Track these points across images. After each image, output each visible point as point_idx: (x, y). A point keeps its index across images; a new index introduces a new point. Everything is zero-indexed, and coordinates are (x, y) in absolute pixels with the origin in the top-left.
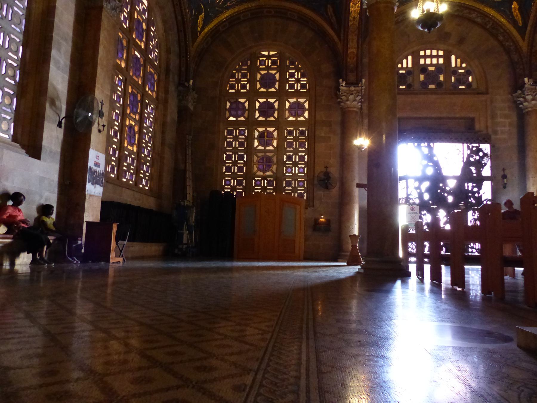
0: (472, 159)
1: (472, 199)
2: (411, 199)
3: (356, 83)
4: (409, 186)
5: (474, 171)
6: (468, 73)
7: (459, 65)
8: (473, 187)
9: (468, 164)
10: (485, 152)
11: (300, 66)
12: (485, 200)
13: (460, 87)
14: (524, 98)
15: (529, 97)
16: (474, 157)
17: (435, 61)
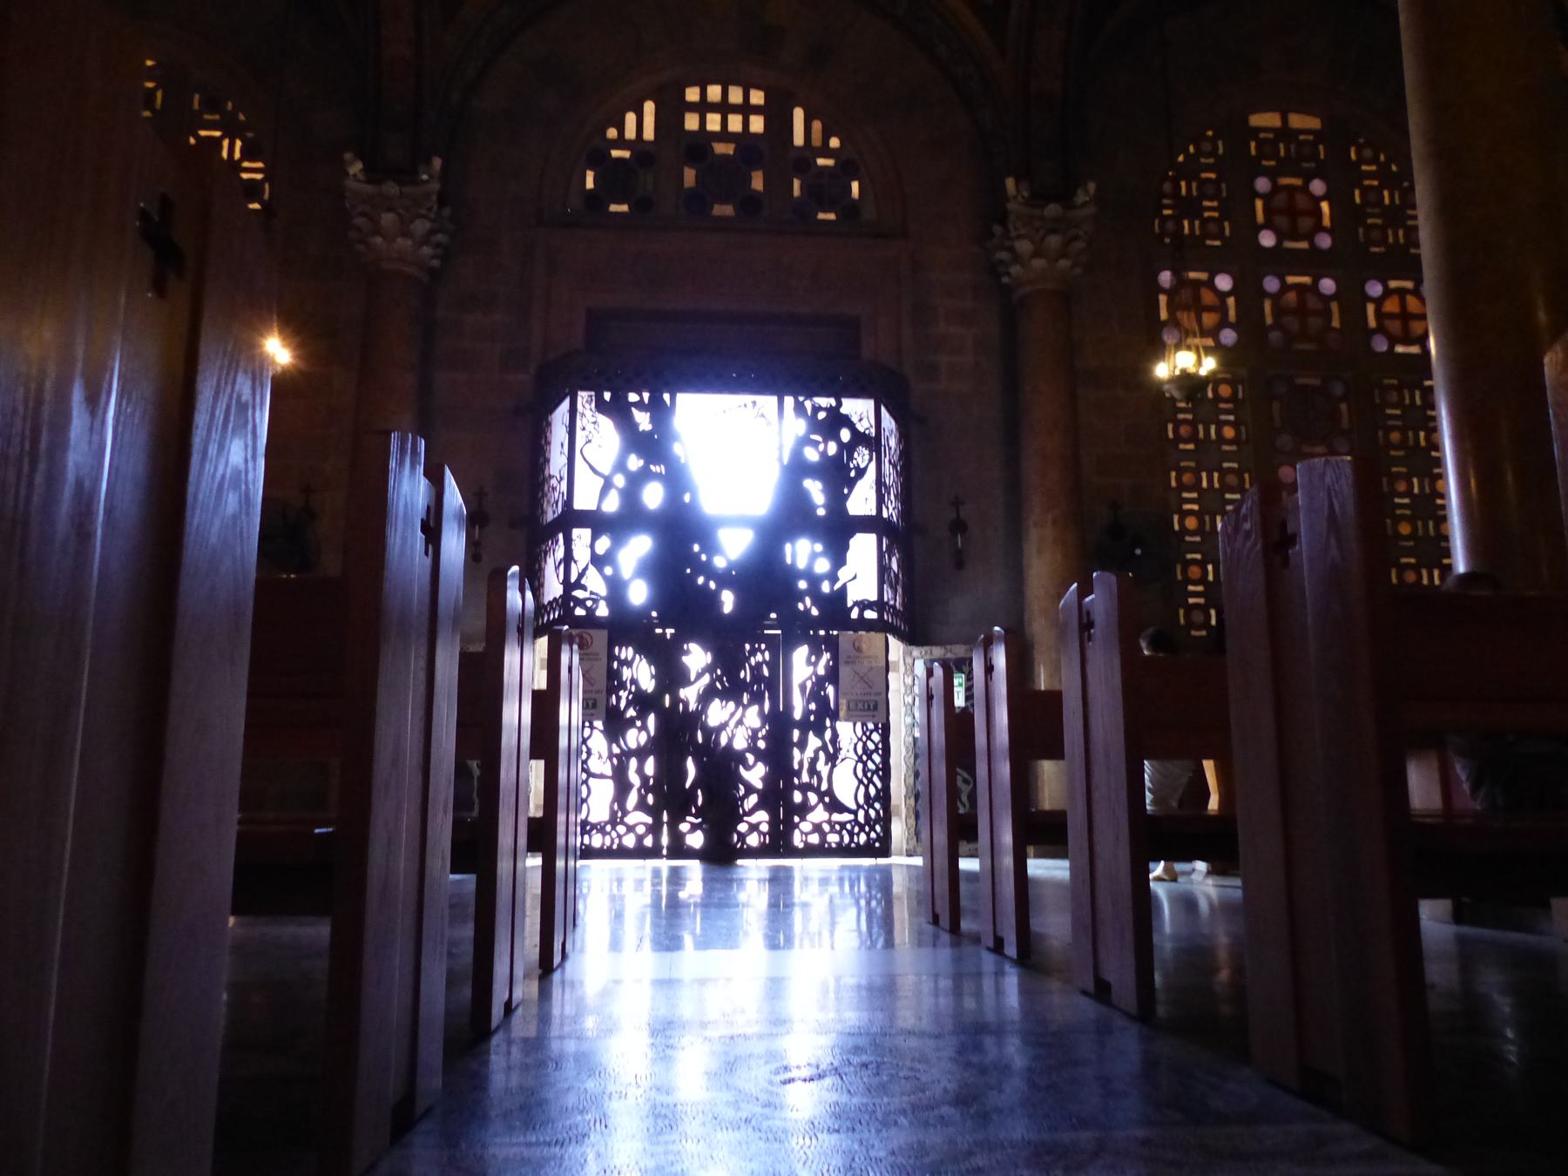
0: (812, 455)
1: (808, 601)
2: (581, 603)
3: (406, 174)
4: (576, 555)
6: (847, 167)
7: (817, 140)
8: (814, 556)
9: (797, 469)
10: (861, 428)
11: (242, 117)
12: (856, 604)
13: (821, 216)
14: (1011, 249)
15: (1024, 246)
16: (821, 447)
17: (735, 122)
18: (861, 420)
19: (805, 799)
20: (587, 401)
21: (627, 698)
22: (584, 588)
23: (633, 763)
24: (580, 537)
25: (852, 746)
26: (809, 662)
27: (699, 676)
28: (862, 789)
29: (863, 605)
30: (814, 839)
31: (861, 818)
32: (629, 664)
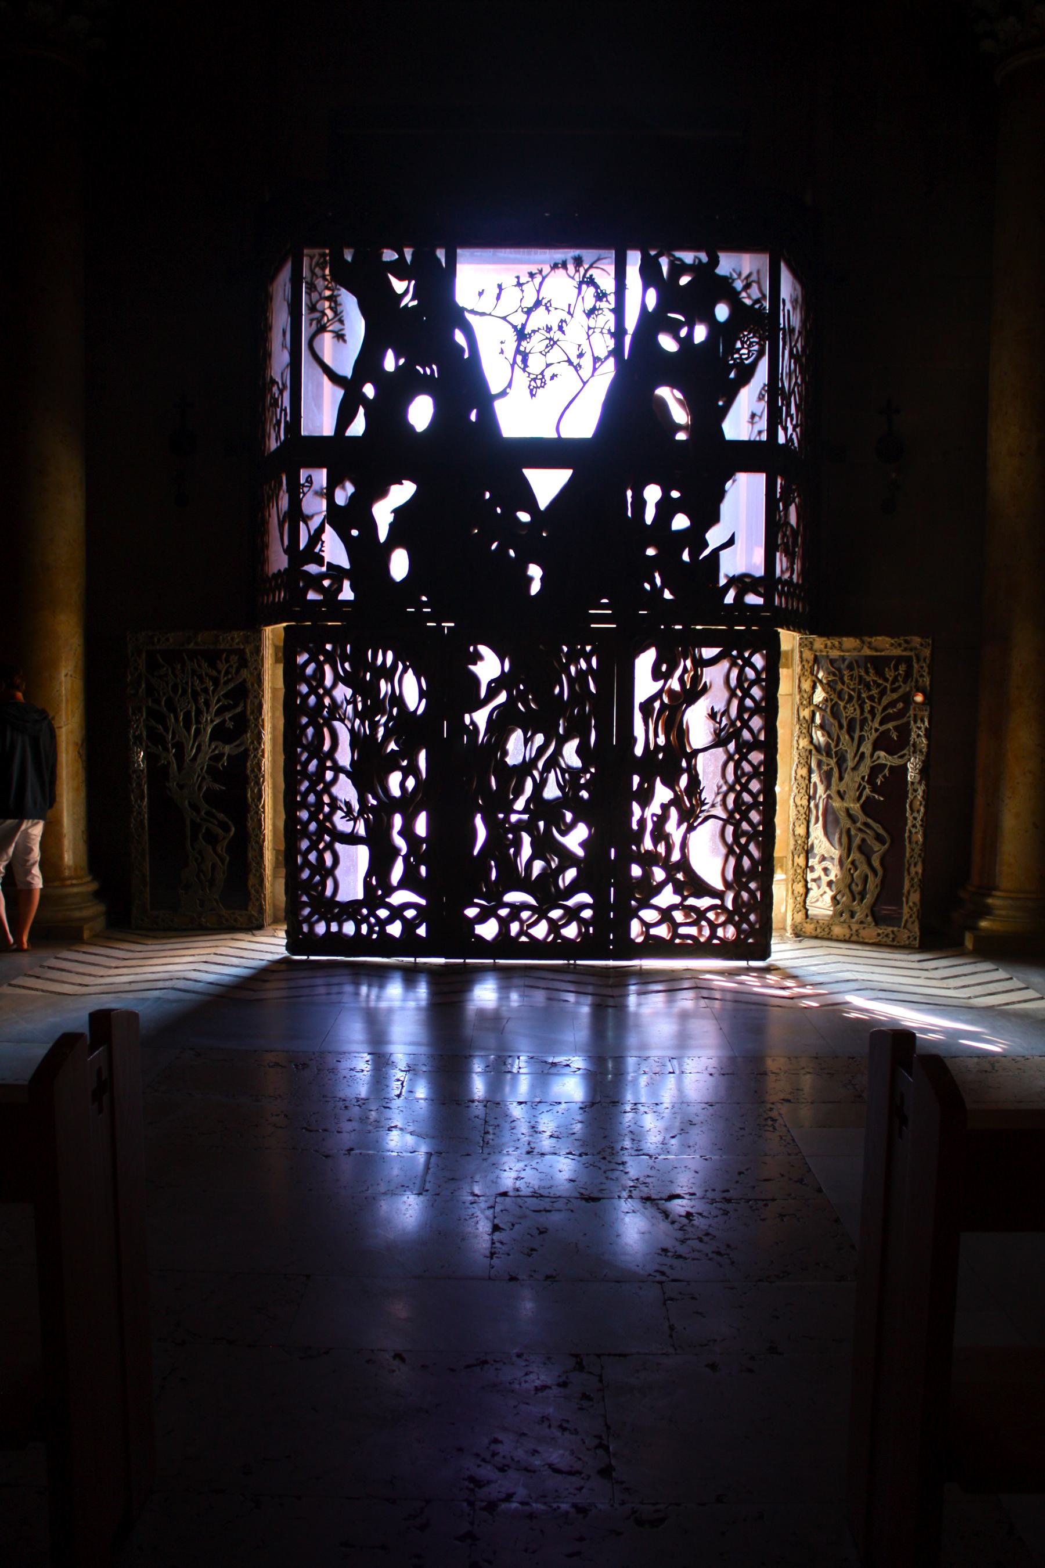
2: (315, 582)
5: (680, 416)
8: (667, 509)
12: (732, 581)
16: (683, 332)
18: (747, 287)
19: (648, 875)
20: (317, 264)
21: (386, 724)
22: (319, 560)
23: (398, 820)
24: (309, 479)
25: (719, 798)
26: (657, 674)
27: (492, 693)
28: (732, 861)
29: (743, 583)
30: (662, 931)
31: (729, 905)
32: (388, 674)
